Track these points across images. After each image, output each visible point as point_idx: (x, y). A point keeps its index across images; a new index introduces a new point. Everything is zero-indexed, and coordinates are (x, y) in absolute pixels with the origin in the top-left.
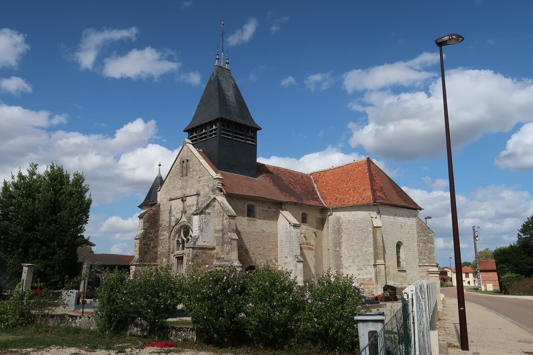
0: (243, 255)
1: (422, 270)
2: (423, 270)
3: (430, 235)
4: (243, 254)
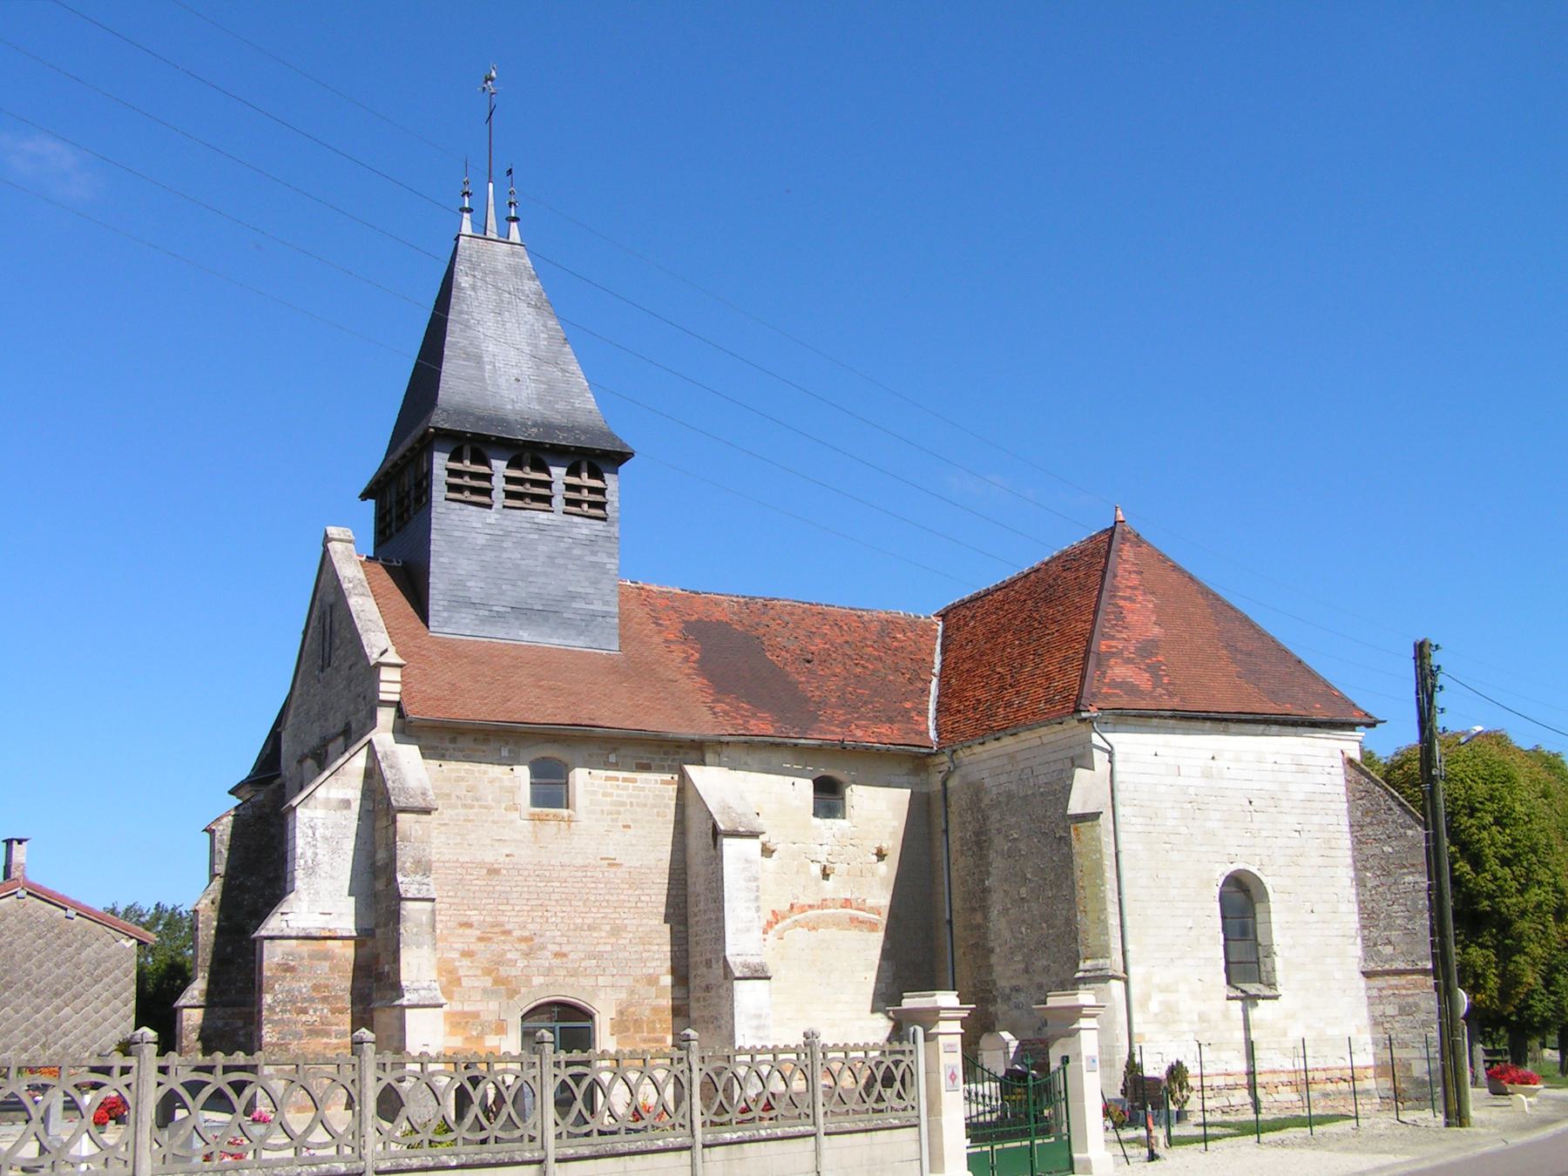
0: (510, 960)
1: (1380, 990)
2: (1385, 993)
3: (1410, 832)
4: (509, 956)
